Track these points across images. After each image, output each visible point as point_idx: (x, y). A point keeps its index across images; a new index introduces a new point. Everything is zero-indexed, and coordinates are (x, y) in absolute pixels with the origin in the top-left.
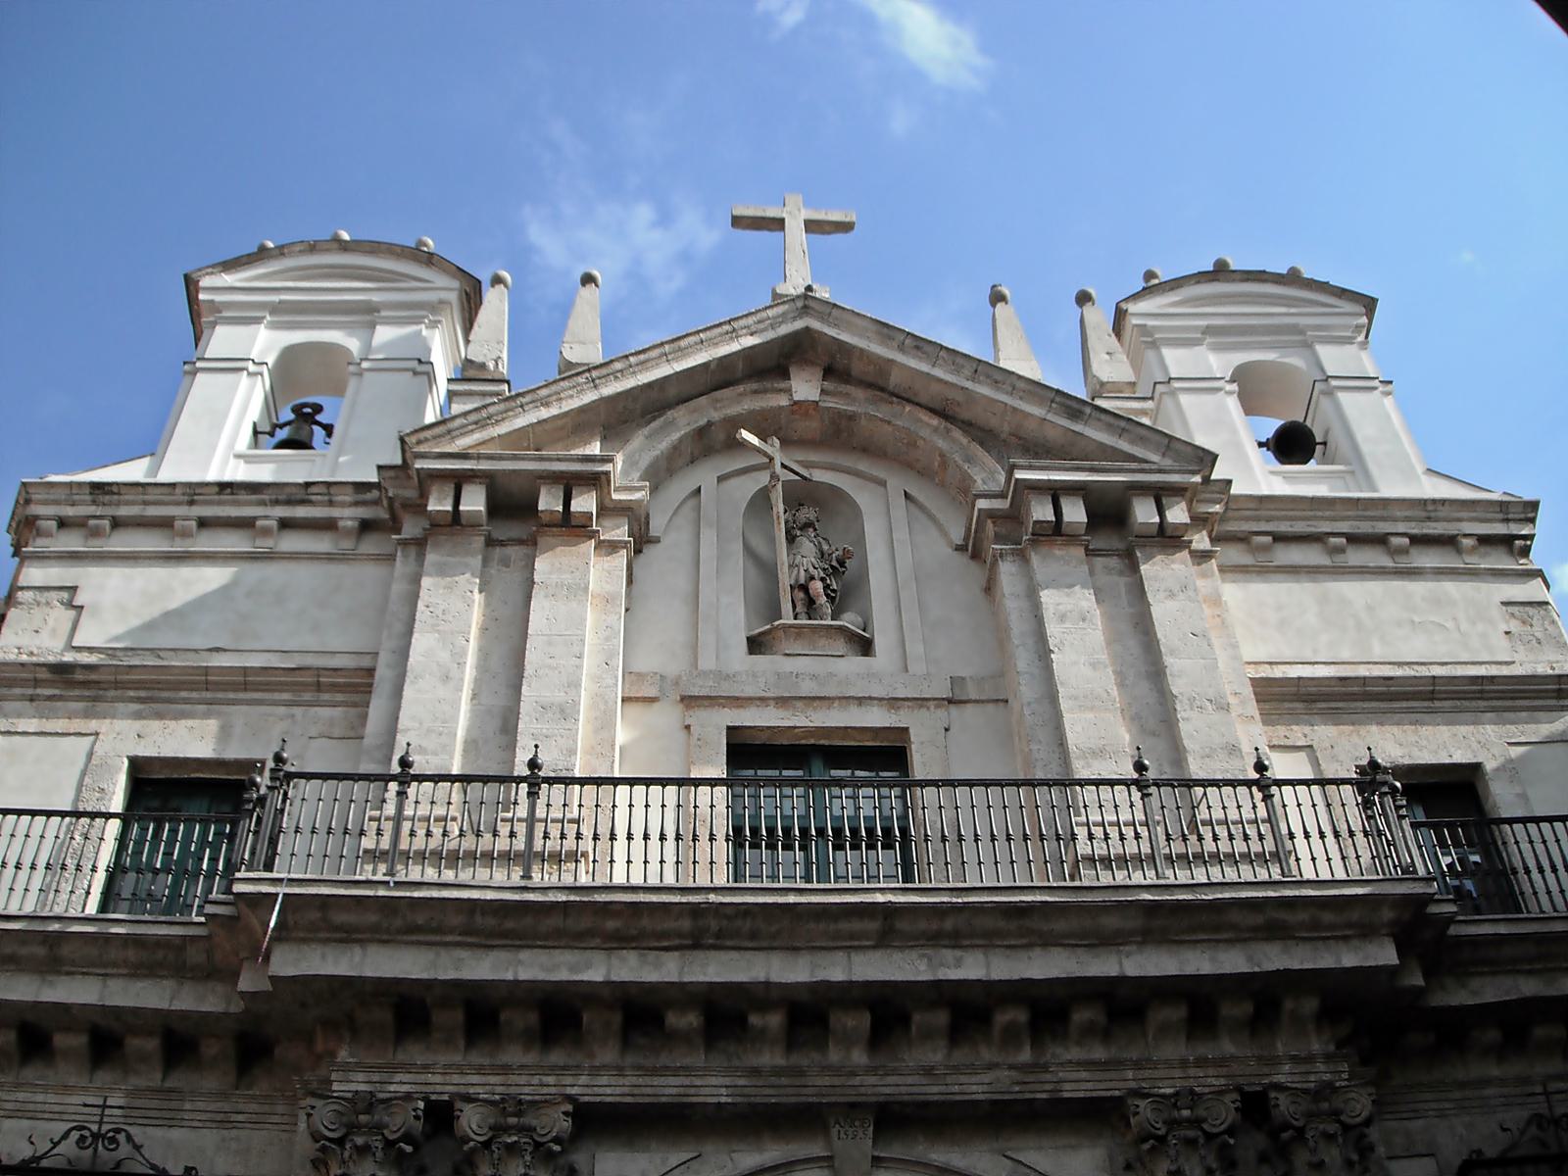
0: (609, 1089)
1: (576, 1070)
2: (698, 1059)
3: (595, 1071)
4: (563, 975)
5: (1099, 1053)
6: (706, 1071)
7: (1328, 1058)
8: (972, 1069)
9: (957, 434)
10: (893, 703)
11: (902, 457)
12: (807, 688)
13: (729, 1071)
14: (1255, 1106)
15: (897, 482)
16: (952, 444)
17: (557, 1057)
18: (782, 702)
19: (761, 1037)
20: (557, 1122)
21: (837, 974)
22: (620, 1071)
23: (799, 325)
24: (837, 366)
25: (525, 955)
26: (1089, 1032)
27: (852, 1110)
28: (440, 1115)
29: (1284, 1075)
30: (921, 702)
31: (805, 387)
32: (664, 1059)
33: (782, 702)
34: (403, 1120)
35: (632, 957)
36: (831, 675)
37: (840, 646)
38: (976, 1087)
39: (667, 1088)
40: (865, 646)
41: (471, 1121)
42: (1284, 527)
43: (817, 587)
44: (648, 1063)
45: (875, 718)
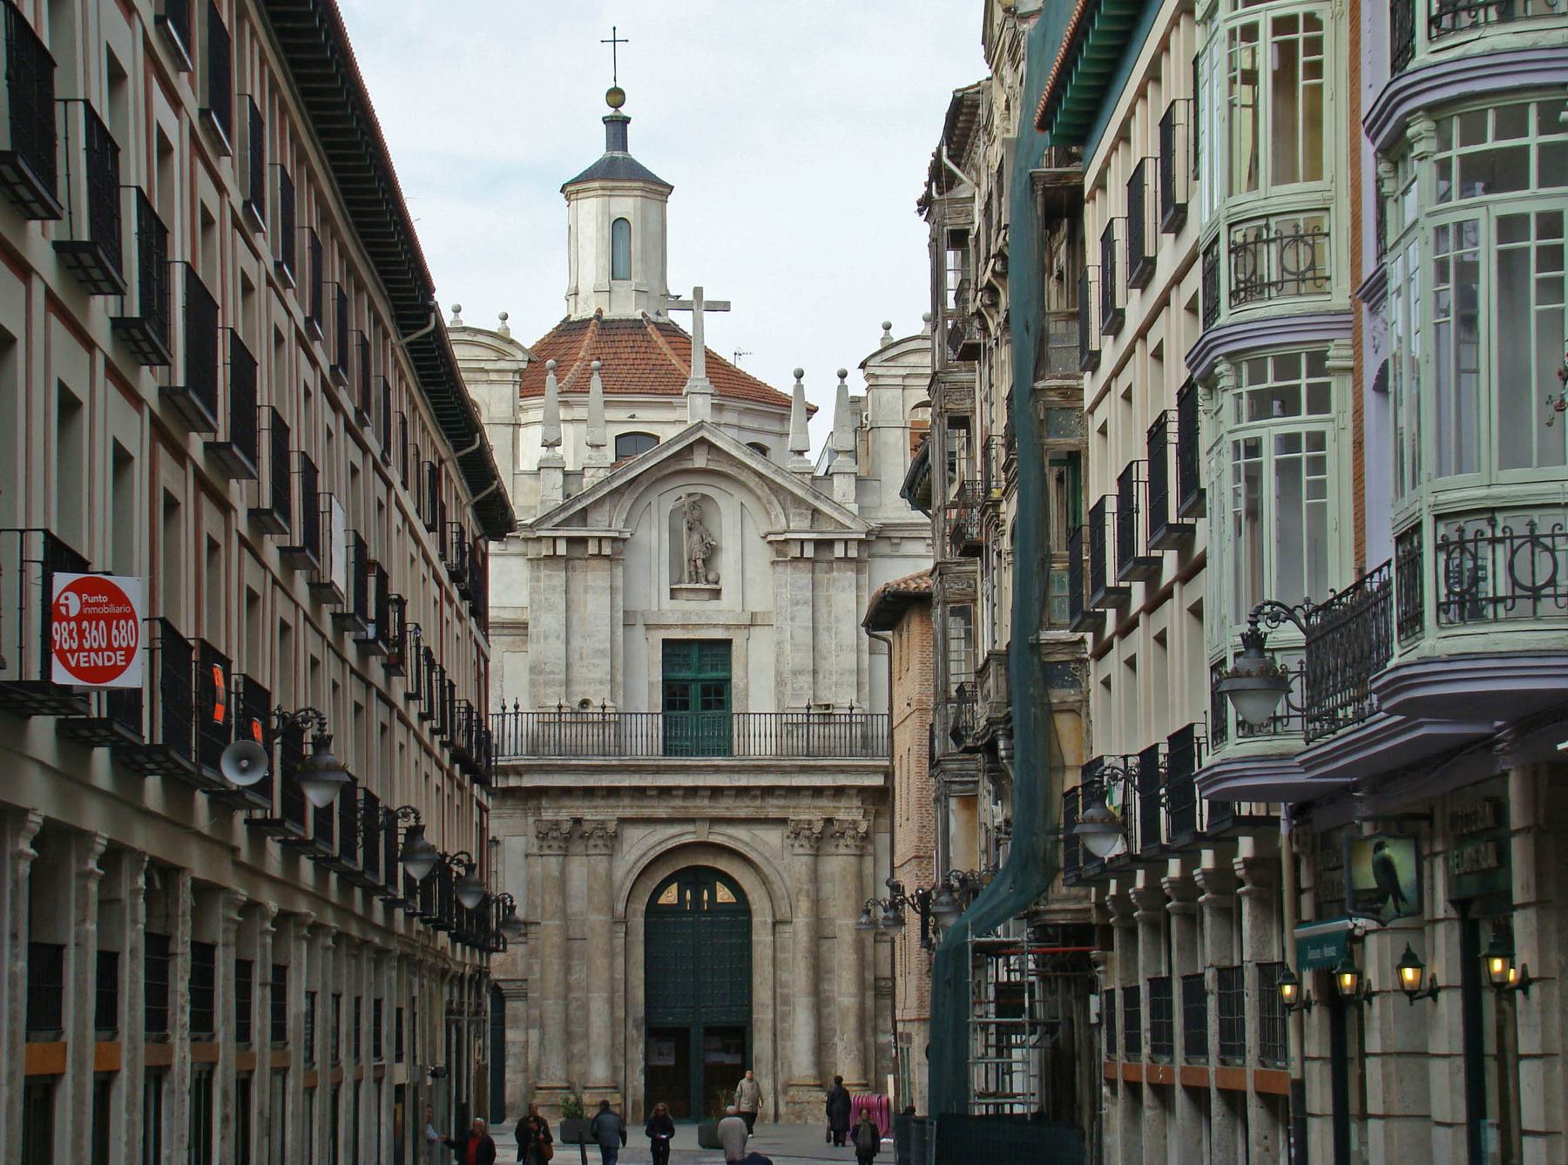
0: (629, 813)
1: (618, 807)
2: (655, 803)
3: (624, 807)
4: (616, 784)
5: (782, 802)
6: (658, 807)
7: (858, 808)
8: (741, 807)
9: (766, 489)
10: (727, 627)
11: (743, 485)
12: (694, 620)
13: (667, 807)
14: (829, 821)
15: (739, 496)
16: (763, 491)
17: (612, 802)
18: (684, 626)
19: (677, 796)
20: (612, 827)
21: (701, 784)
22: (632, 807)
23: (698, 435)
24: (712, 447)
25: (604, 777)
26: (781, 796)
27: (703, 819)
28: (578, 821)
29: (841, 816)
30: (738, 626)
31: (700, 460)
32: (645, 803)
33: (684, 626)
34: (566, 827)
35: (637, 777)
36: (704, 612)
37: (706, 596)
38: (742, 813)
39: (647, 813)
40: (716, 594)
41: (587, 827)
42: (906, 534)
43: (699, 563)
44: (641, 804)
45: (719, 634)
